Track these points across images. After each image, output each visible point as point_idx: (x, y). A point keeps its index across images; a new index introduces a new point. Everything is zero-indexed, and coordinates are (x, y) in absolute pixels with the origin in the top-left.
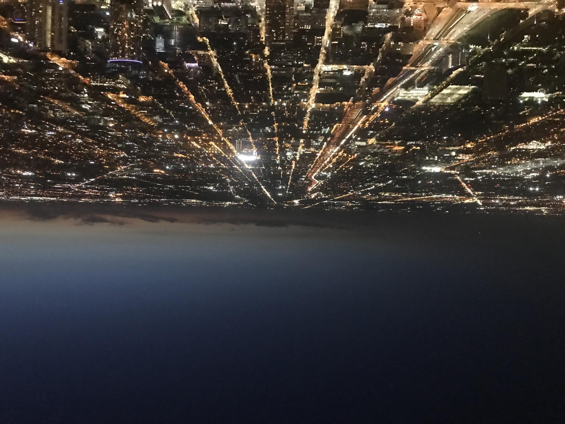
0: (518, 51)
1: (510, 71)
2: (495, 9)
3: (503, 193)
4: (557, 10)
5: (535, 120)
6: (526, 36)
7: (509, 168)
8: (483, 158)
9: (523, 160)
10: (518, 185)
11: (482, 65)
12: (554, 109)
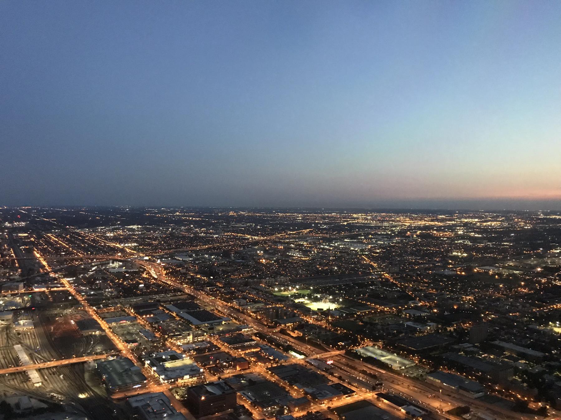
4: (548, 407)
12: (543, 313)
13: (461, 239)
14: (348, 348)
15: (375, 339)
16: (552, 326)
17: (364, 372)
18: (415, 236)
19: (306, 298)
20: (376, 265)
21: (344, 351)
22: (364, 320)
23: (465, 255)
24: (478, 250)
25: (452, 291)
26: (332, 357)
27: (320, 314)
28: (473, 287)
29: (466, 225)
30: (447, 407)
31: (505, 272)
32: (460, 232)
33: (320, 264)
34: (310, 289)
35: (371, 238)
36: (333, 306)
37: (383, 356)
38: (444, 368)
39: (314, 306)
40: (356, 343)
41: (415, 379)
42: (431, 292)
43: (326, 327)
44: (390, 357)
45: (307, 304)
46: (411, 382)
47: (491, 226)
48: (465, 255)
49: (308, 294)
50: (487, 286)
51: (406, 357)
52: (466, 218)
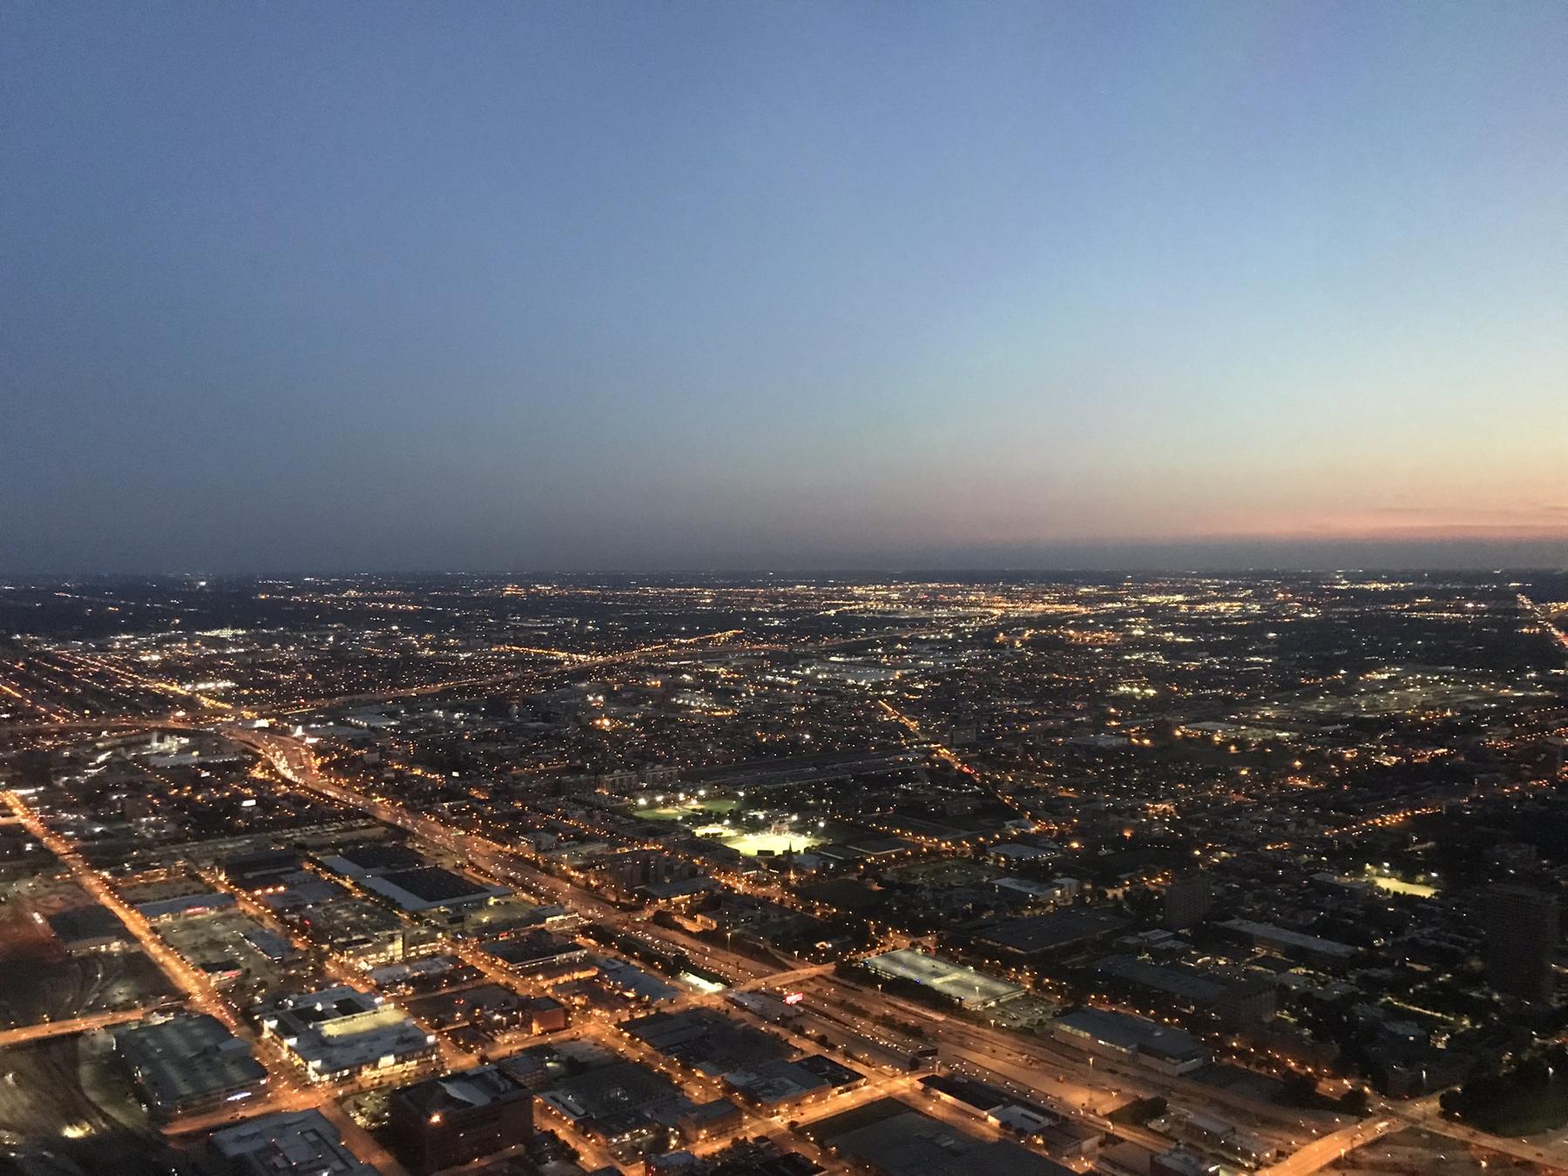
0: (1459, 1013)
1: (1476, 964)
2: (1536, 1144)
3: (1456, 628)
5: (1392, 820)
6: (1440, 1046)
7: (1447, 698)
8: (1530, 729)
9: (1411, 717)
10: (1417, 649)
11: (1560, 1000)
12: (1349, 841)
13: (1138, 651)
14: (843, 956)
15: (916, 930)
16: (1371, 875)
17: (887, 1022)
18: (1018, 644)
19: (727, 822)
20: (913, 725)
21: (831, 967)
22: (886, 877)
23: (1151, 692)
24: (1184, 678)
25: (1117, 791)
26: (800, 983)
27: (764, 866)
28: (1173, 779)
29: (1151, 611)
30: (1109, 1103)
31: (1254, 735)
32: (1139, 632)
33: (764, 728)
34: (736, 797)
35: (902, 652)
36: (800, 843)
37: (937, 974)
38: (1100, 1000)
39: (749, 845)
40: (864, 941)
41: (1024, 1033)
42: (1064, 794)
43: (782, 901)
44: (956, 976)
45: (728, 839)
46: (1011, 1039)
47: (1217, 612)
48: (1151, 692)
49: (731, 812)
50: (1210, 775)
51: (997, 974)
52: (1152, 592)
